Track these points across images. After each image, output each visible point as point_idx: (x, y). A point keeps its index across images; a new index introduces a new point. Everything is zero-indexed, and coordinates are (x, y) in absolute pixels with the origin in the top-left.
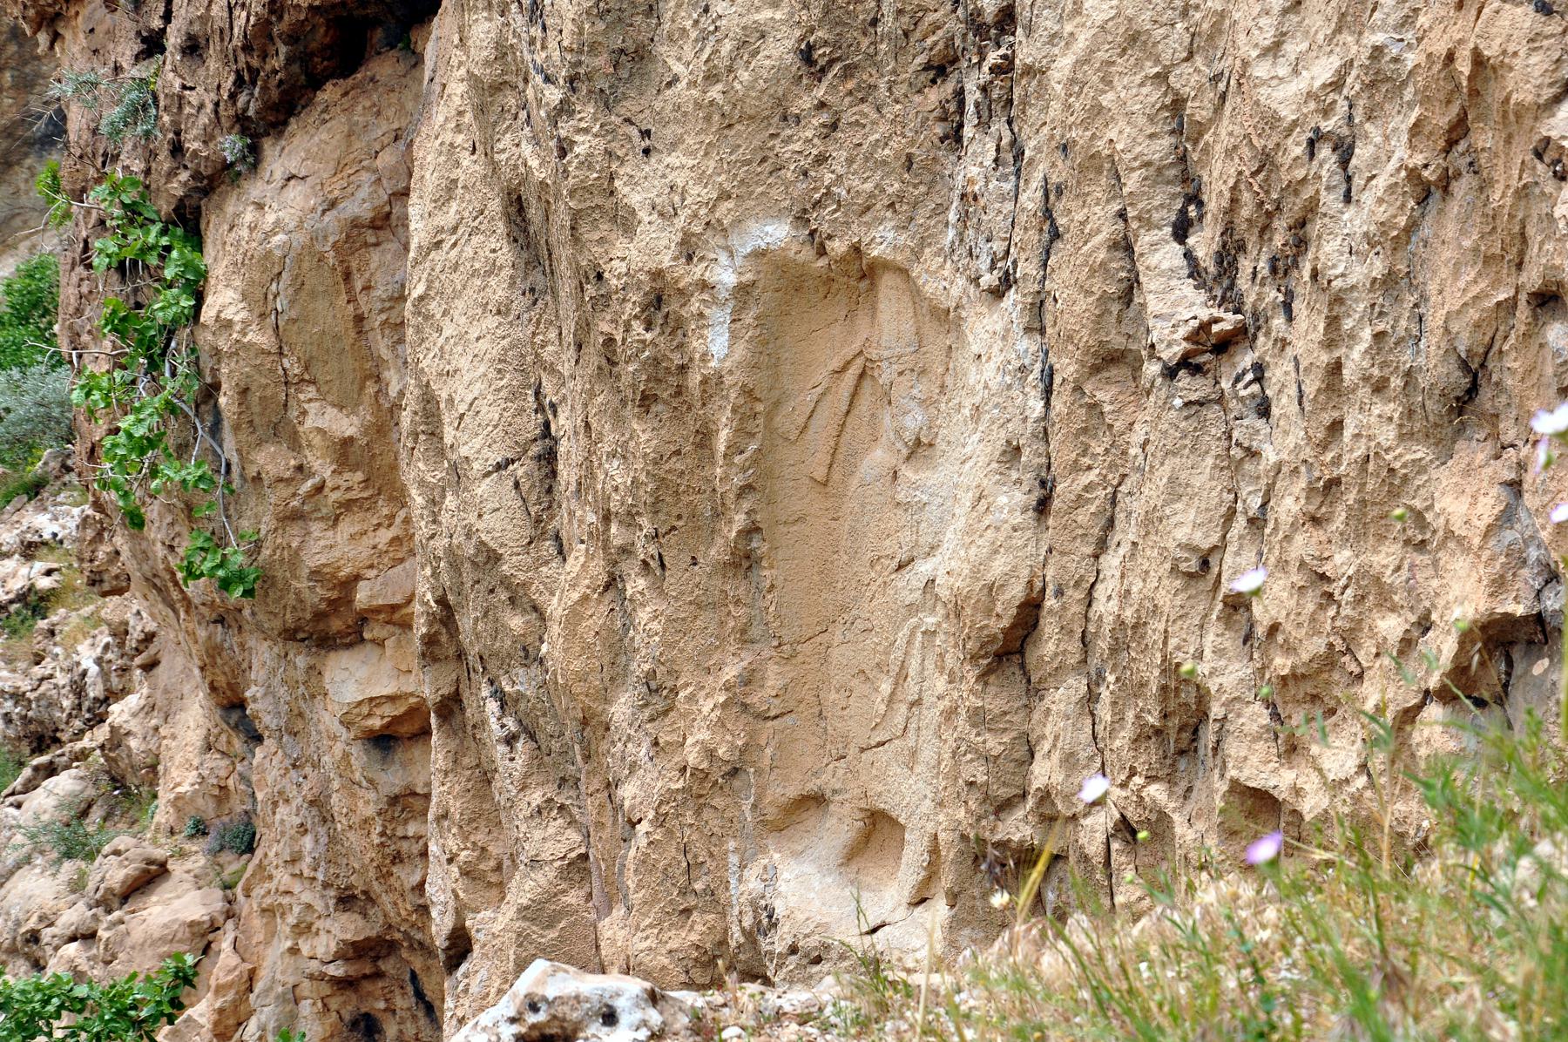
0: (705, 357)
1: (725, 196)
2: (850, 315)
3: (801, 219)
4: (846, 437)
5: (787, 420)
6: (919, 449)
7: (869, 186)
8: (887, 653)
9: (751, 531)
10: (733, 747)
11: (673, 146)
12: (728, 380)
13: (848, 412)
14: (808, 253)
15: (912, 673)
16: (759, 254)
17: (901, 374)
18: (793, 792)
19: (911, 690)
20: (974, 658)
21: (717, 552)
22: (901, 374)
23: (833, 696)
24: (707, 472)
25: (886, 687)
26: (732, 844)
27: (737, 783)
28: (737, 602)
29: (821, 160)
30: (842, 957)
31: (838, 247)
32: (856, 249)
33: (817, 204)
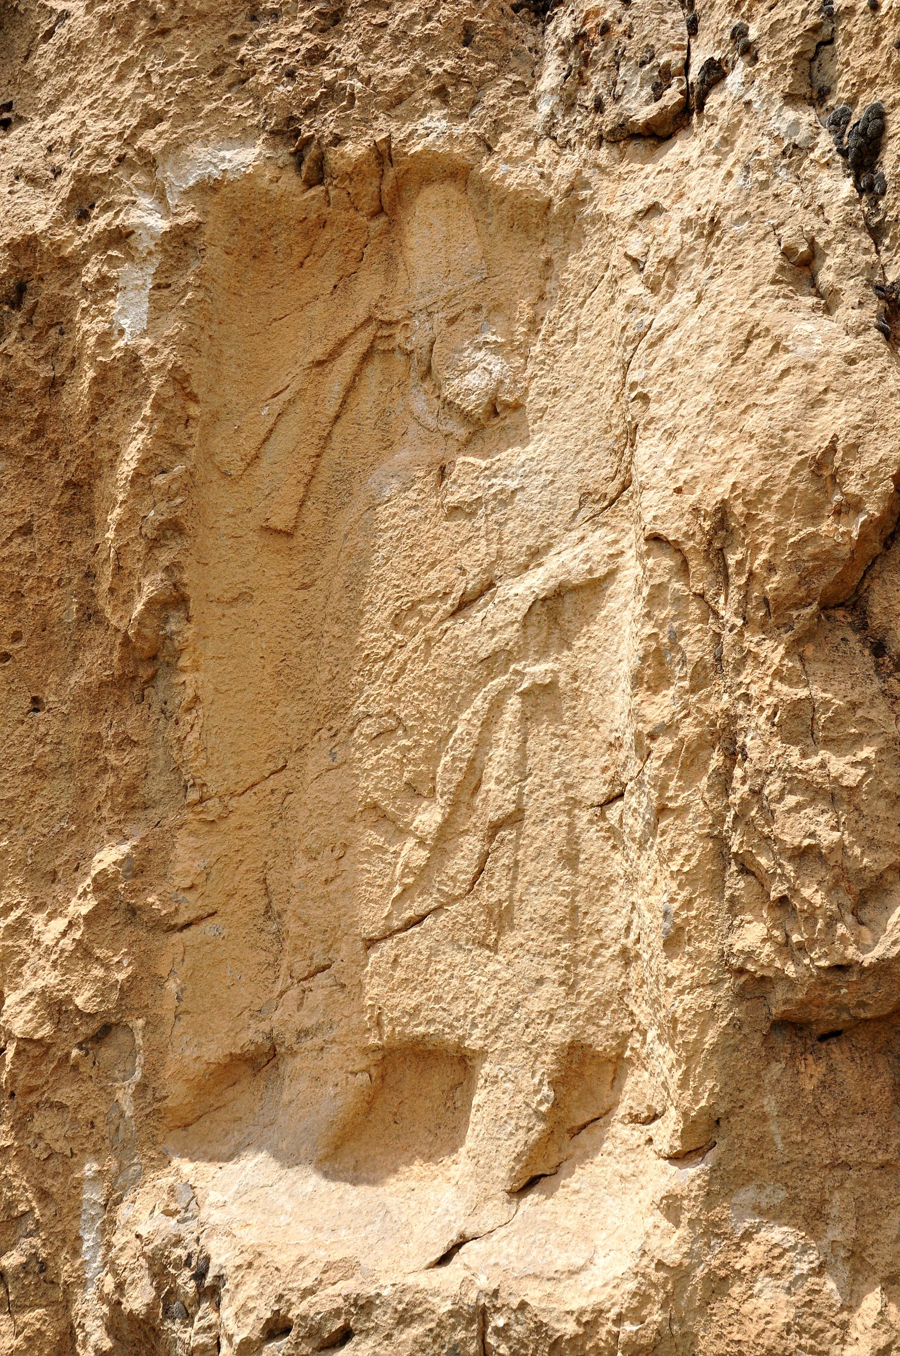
0: (104, 340)
1: (152, 119)
2: (345, 281)
3: (286, 132)
4: (332, 456)
5: (229, 449)
6: (496, 419)
7: (402, 70)
8: (432, 758)
9: (174, 601)
10: (104, 988)
11: (52, 106)
12: (147, 363)
13: (337, 417)
14: (290, 182)
15: (493, 770)
16: (208, 188)
17: (452, 321)
18: (215, 1051)
19: (495, 798)
20: (772, 614)
21: (96, 662)
22: (452, 321)
23: (303, 866)
24: (80, 548)
25: (428, 817)
26: (90, 1168)
27: (107, 1053)
28: (125, 742)
29: (316, 56)
30: (404, 1319)
31: (354, 150)
32: (383, 155)
33: (312, 109)
